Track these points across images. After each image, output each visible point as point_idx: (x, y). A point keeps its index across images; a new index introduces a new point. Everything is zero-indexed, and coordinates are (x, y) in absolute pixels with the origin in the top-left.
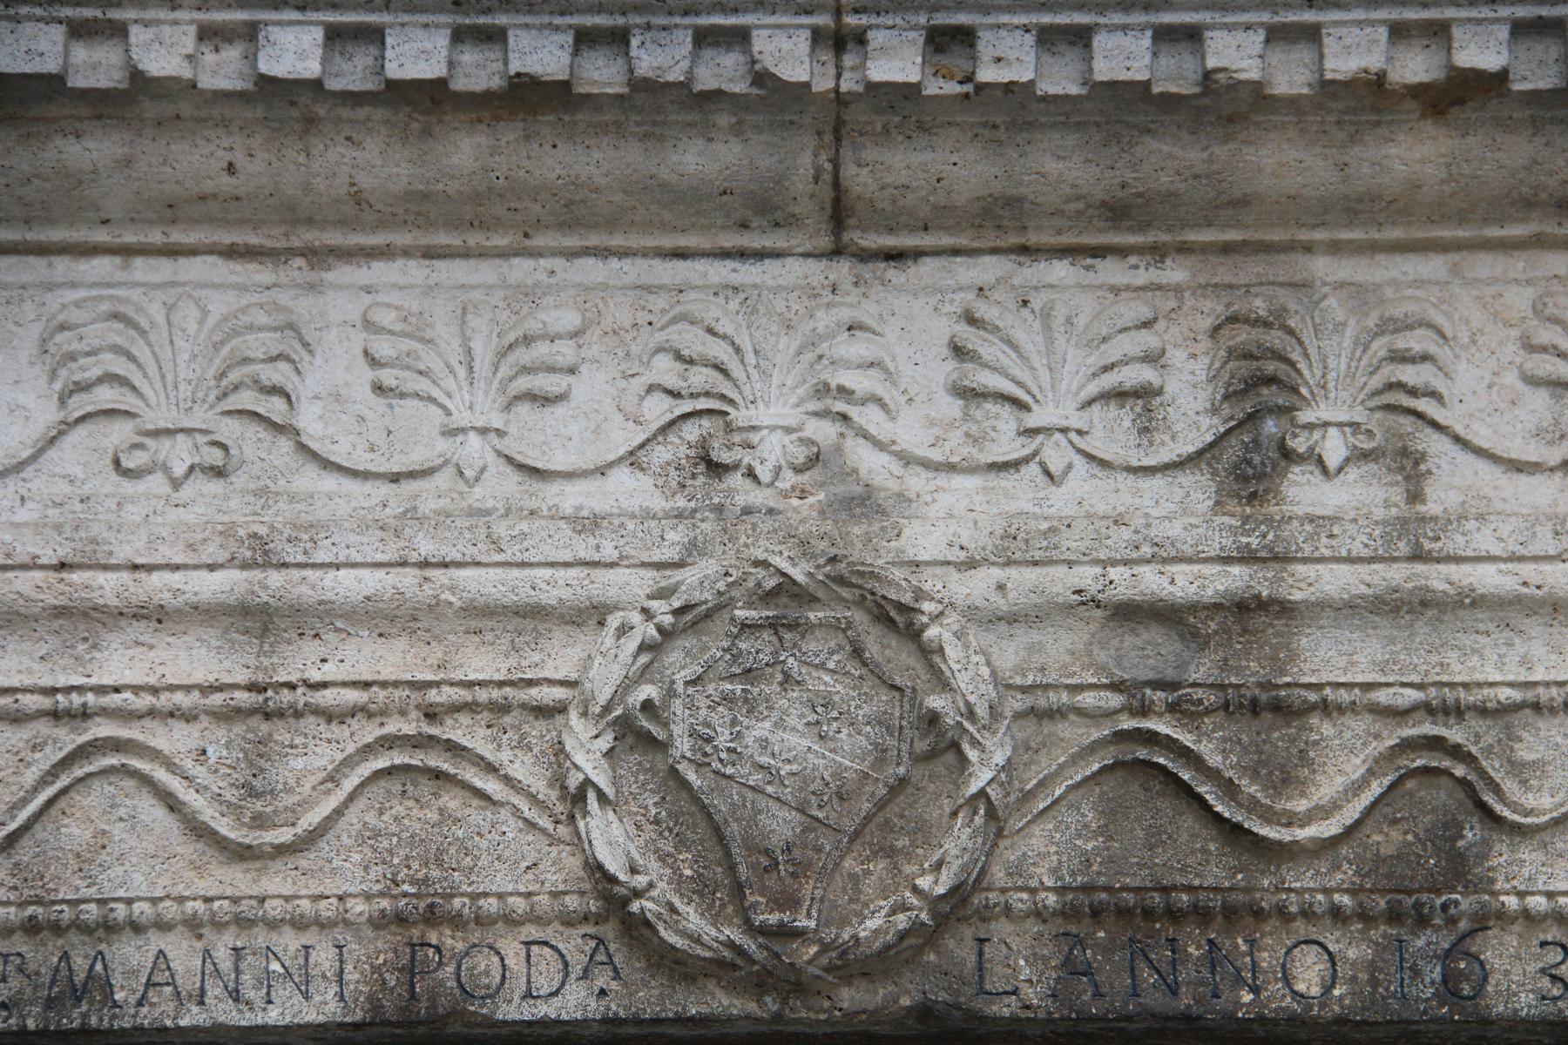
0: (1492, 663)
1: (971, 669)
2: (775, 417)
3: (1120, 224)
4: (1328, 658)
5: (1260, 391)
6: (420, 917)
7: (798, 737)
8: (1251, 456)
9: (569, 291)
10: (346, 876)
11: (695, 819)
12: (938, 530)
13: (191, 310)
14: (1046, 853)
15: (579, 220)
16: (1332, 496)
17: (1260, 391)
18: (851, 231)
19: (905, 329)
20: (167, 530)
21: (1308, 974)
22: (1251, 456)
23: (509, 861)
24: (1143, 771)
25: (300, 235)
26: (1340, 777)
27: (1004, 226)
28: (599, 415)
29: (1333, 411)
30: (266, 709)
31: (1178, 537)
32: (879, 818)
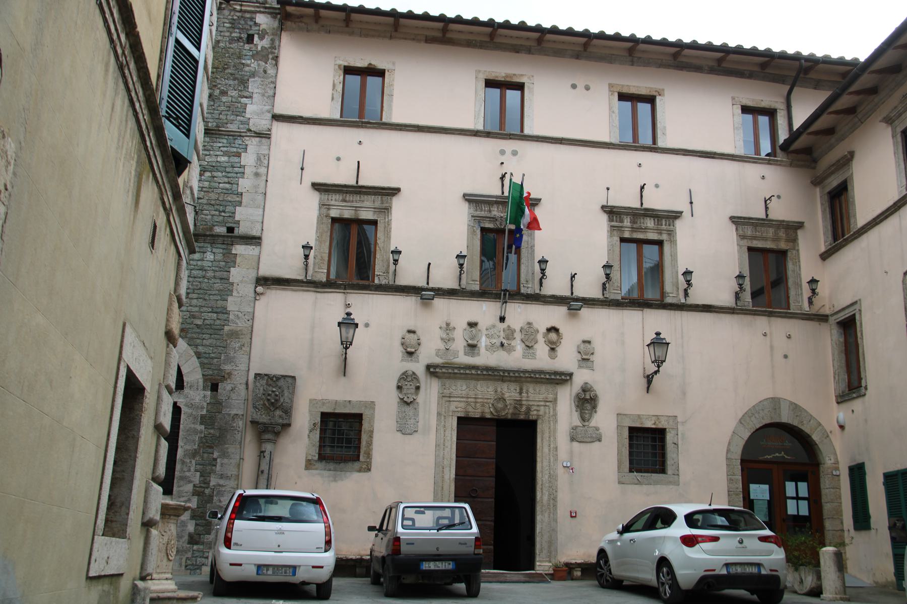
0: (531, 403)
1: (508, 402)
2: (499, 390)
3: (515, 381)
4: (524, 403)
5: (521, 389)
6: (483, 413)
7: (500, 405)
8: (521, 393)
9: (490, 383)
10: (479, 410)
11: (495, 409)
12: (507, 395)
13: (473, 382)
14: (511, 411)
15: (490, 380)
16: (524, 395)
17: (521, 389)
18: (503, 381)
19: (505, 386)
20: (472, 394)
21: (522, 417)
22: (521, 393)
23: (487, 410)
24: (515, 408)
25: (478, 380)
26: (524, 409)
27: (510, 381)
28: (491, 389)
29: (524, 391)
30: (476, 402)
31: (516, 396)
32: (504, 409)
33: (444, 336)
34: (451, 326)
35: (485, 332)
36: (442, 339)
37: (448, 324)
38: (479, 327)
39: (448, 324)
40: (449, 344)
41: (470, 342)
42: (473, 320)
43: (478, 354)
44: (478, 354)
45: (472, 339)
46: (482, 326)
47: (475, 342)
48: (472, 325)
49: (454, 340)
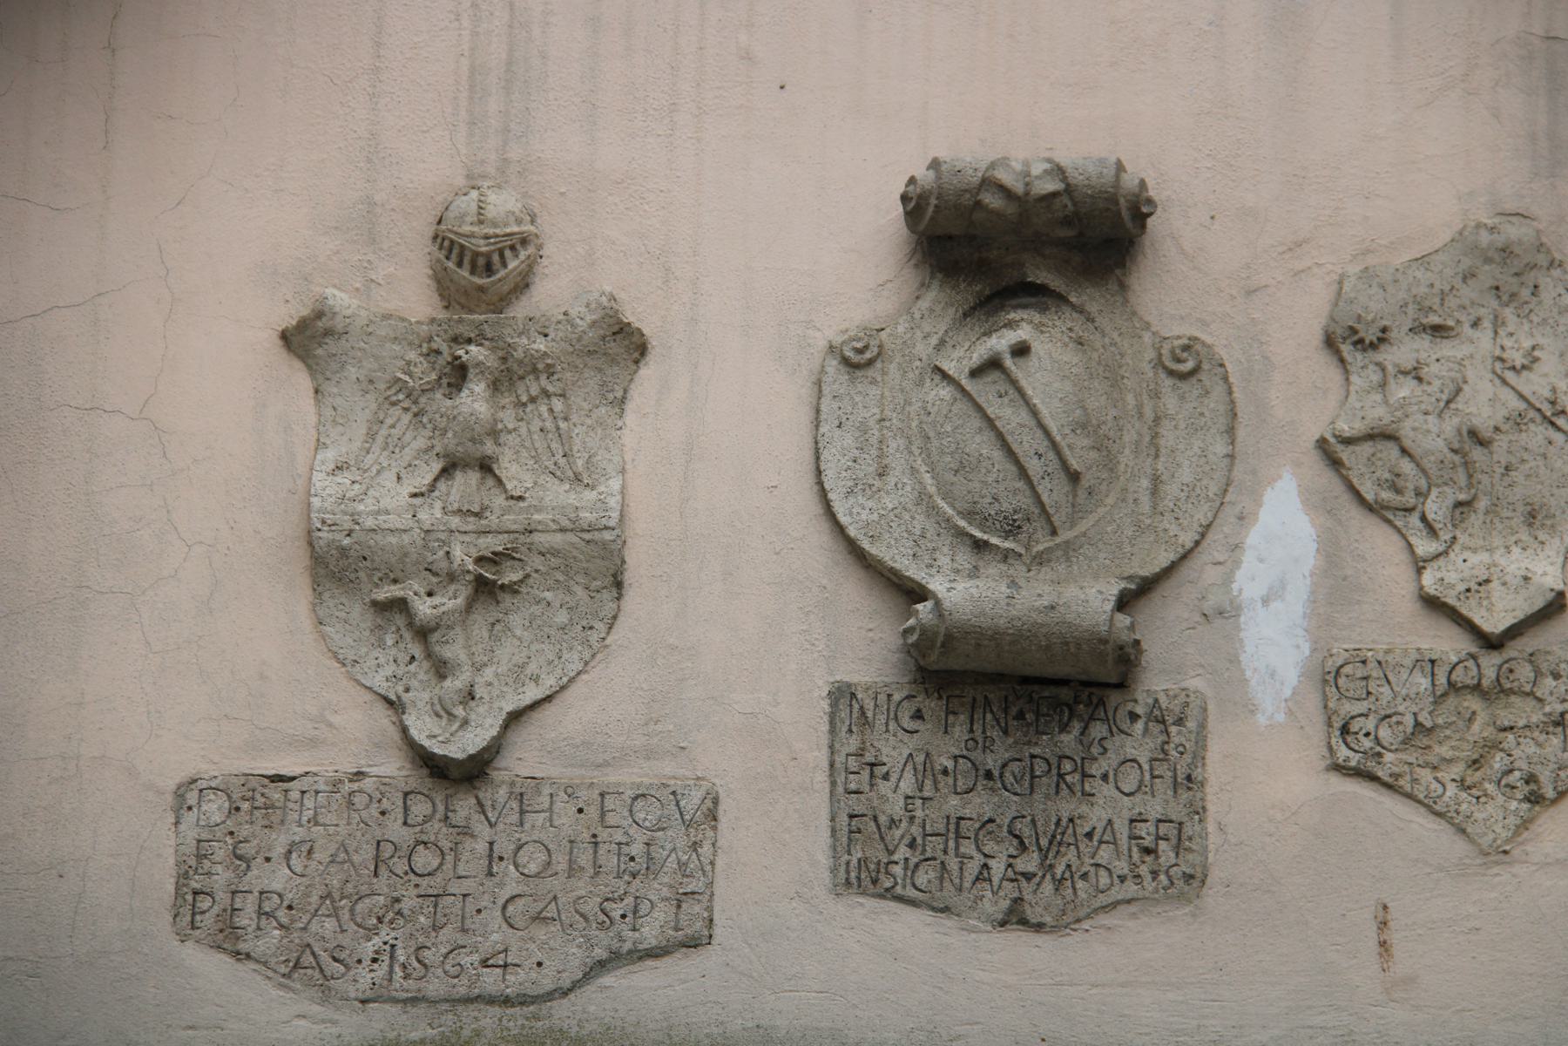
33: (392, 497)
34: (558, 293)
35: (1303, 399)
36: (338, 566)
37: (479, 270)
38: (1176, 289)
39: (479, 270)
40: (502, 661)
41: (963, 591)
42: (1031, 134)
43: (1169, 862)
44: (1169, 862)
45: (987, 536)
46: (1237, 267)
47: (1086, 599)
48: (1020, 248)
49: (603, 568)
